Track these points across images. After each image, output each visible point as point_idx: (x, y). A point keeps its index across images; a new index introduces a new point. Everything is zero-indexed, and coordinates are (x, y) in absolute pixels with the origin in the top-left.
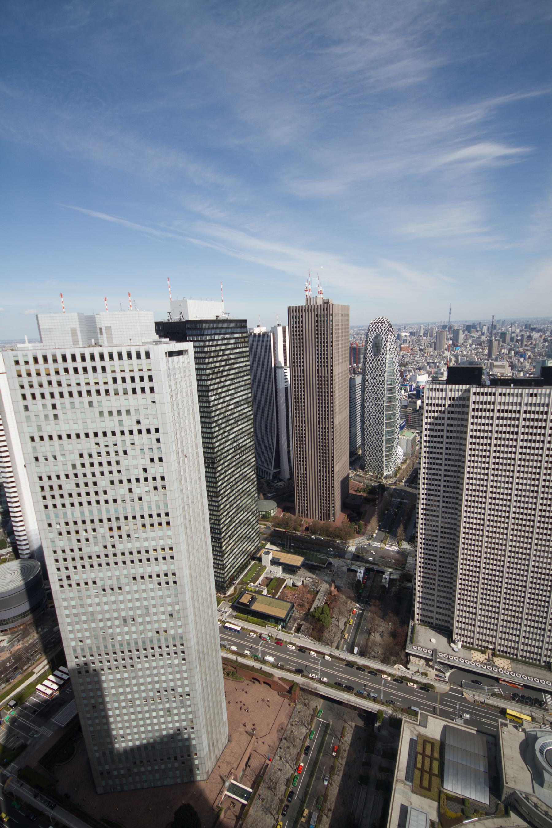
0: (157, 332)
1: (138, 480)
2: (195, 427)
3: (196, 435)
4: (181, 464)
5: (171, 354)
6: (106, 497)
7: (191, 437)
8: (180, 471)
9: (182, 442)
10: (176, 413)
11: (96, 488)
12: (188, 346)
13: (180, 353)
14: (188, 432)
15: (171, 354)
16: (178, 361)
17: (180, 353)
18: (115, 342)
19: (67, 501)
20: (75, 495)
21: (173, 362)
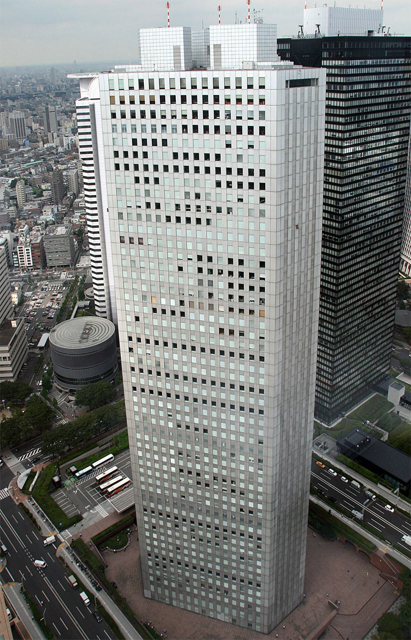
2: (315, 188)
3: (315, 200)
4: (290, 238)
5: (293, 84)
9: (294, 207)
10: (291, 165)
12: (320, 74)
14: (304, 195)
15: (293, 84)
16: (303, 95)
18: (224, 65)
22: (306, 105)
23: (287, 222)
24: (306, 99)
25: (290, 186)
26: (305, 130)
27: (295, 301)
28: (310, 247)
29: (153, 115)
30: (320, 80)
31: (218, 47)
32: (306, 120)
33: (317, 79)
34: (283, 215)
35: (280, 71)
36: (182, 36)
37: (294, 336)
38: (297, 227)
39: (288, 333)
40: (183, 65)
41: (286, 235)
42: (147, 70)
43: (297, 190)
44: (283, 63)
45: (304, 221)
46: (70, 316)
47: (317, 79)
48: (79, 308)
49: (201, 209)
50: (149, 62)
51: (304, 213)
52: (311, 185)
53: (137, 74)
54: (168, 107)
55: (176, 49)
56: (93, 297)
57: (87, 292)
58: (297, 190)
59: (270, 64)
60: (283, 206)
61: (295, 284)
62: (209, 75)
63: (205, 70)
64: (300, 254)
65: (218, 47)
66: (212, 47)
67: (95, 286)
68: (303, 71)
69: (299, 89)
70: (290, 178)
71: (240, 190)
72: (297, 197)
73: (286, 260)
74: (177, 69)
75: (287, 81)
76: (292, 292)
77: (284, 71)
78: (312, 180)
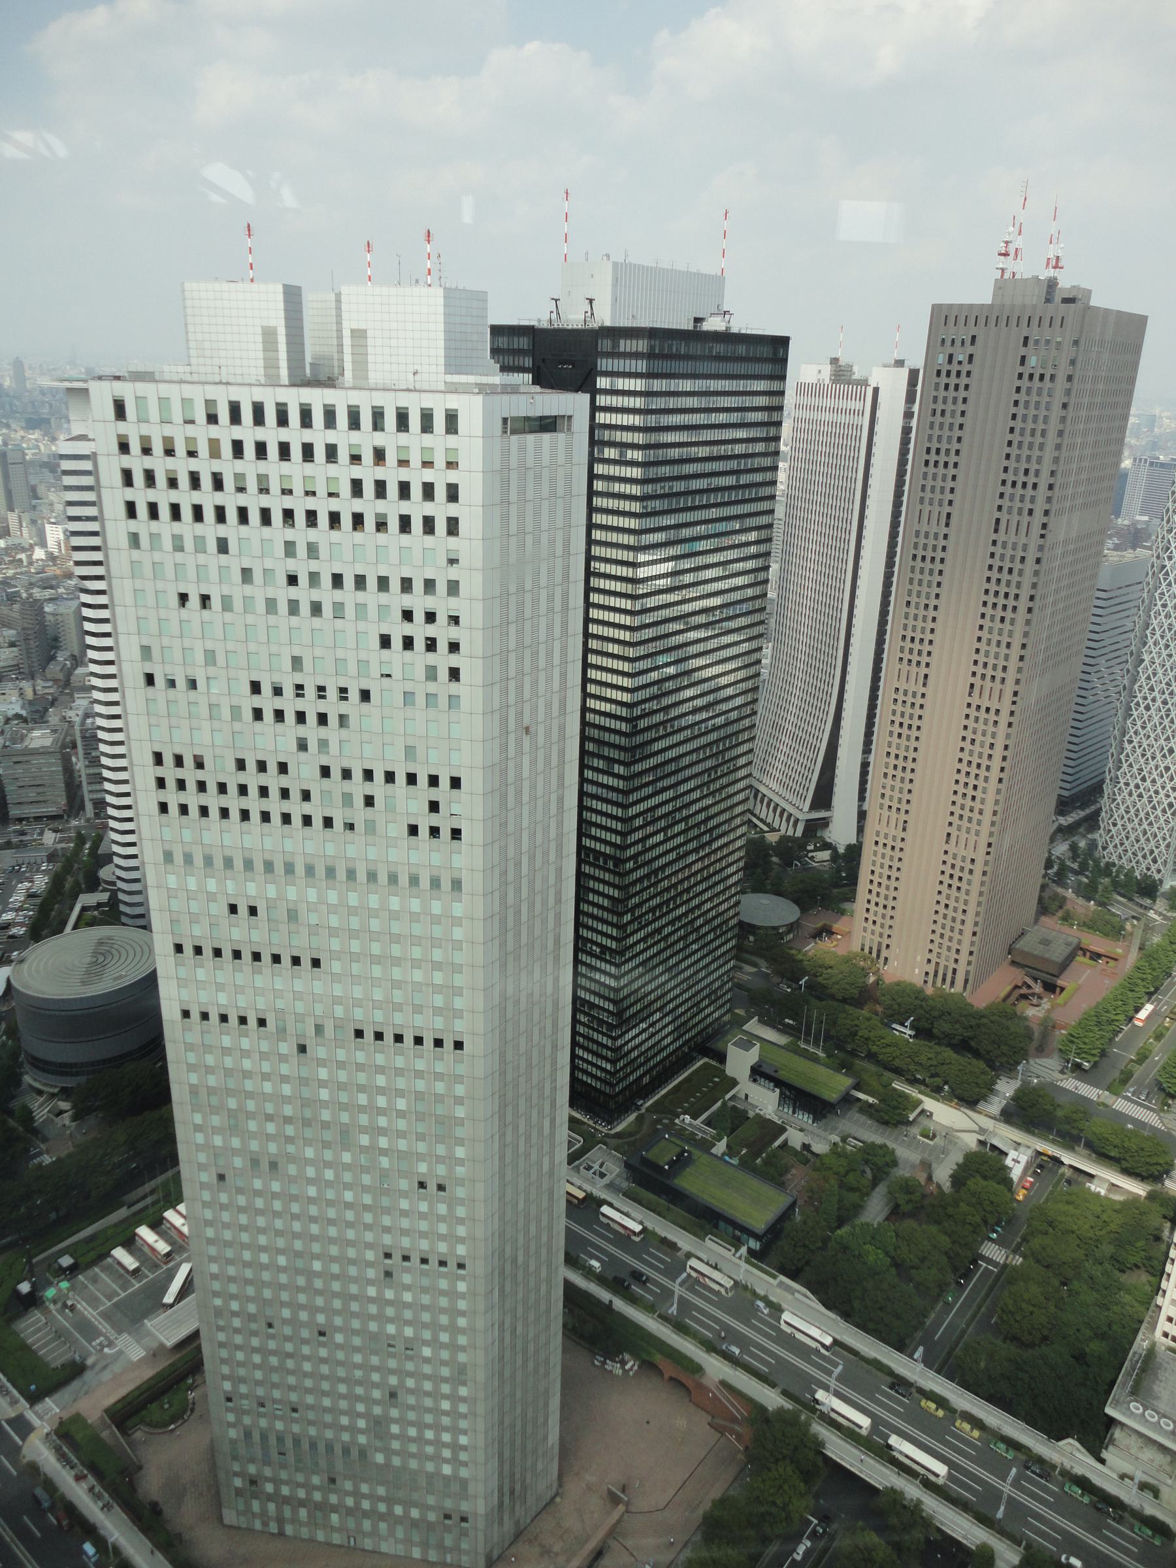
0: (495, 352)
1: (390, 777)
3: (564, 675)
6: (307, 809)
7: (549, 679)
8: (504, 773)
9: (520, 688)
11: (284, 781)
12: (574, 404)
13: (548, 424)
14: (542, 663)
16: (538, 448)
17: (548, 424)
18: (374, 378)
19: (213, 801)
20: (232, 789)
22: (546, 474)
23: (504, 720)
24: (546, 461)
26: (545, 525)
27: (525, 881)
28: (554, 773)
29: (218, 484)
30: (575, 421)
31: (359, 335)
32: (545, 504)
33: (570, 417)
34: (497, 706)
35: (491, 397)
36: (281, 306)
37: (524, 952)
38: (527, 729)
39: (510, 946)
40: (284, 373)
41: (504, 748)
42: (203, 379)
43: (527, 653)
44: (497, 379)
45: (541, 717)
46: (64, 923)
47: (570, 417)
48: (84, 909)
49: (328, 693)
50: (208, 361)
51: (541, 702)
53: (176, 386)
54: (249, 465)
55: (269, 335)
56: (114, 884)
57: (105, 873)
58: (527, 653)
60: (497, 688)
62: (340, 399)
63: (334, 386)
64: (533, 787)
65: (359, 335)
66: (346, 333)
67: (116, 860)
68: (538, 398)
69: (531, 438)
70: (512, 629)
71: (408, 653)
72: (527, 669)
73: (504, 797)
74: (272, 381)
76: (518, 865)
77: (497, 398)
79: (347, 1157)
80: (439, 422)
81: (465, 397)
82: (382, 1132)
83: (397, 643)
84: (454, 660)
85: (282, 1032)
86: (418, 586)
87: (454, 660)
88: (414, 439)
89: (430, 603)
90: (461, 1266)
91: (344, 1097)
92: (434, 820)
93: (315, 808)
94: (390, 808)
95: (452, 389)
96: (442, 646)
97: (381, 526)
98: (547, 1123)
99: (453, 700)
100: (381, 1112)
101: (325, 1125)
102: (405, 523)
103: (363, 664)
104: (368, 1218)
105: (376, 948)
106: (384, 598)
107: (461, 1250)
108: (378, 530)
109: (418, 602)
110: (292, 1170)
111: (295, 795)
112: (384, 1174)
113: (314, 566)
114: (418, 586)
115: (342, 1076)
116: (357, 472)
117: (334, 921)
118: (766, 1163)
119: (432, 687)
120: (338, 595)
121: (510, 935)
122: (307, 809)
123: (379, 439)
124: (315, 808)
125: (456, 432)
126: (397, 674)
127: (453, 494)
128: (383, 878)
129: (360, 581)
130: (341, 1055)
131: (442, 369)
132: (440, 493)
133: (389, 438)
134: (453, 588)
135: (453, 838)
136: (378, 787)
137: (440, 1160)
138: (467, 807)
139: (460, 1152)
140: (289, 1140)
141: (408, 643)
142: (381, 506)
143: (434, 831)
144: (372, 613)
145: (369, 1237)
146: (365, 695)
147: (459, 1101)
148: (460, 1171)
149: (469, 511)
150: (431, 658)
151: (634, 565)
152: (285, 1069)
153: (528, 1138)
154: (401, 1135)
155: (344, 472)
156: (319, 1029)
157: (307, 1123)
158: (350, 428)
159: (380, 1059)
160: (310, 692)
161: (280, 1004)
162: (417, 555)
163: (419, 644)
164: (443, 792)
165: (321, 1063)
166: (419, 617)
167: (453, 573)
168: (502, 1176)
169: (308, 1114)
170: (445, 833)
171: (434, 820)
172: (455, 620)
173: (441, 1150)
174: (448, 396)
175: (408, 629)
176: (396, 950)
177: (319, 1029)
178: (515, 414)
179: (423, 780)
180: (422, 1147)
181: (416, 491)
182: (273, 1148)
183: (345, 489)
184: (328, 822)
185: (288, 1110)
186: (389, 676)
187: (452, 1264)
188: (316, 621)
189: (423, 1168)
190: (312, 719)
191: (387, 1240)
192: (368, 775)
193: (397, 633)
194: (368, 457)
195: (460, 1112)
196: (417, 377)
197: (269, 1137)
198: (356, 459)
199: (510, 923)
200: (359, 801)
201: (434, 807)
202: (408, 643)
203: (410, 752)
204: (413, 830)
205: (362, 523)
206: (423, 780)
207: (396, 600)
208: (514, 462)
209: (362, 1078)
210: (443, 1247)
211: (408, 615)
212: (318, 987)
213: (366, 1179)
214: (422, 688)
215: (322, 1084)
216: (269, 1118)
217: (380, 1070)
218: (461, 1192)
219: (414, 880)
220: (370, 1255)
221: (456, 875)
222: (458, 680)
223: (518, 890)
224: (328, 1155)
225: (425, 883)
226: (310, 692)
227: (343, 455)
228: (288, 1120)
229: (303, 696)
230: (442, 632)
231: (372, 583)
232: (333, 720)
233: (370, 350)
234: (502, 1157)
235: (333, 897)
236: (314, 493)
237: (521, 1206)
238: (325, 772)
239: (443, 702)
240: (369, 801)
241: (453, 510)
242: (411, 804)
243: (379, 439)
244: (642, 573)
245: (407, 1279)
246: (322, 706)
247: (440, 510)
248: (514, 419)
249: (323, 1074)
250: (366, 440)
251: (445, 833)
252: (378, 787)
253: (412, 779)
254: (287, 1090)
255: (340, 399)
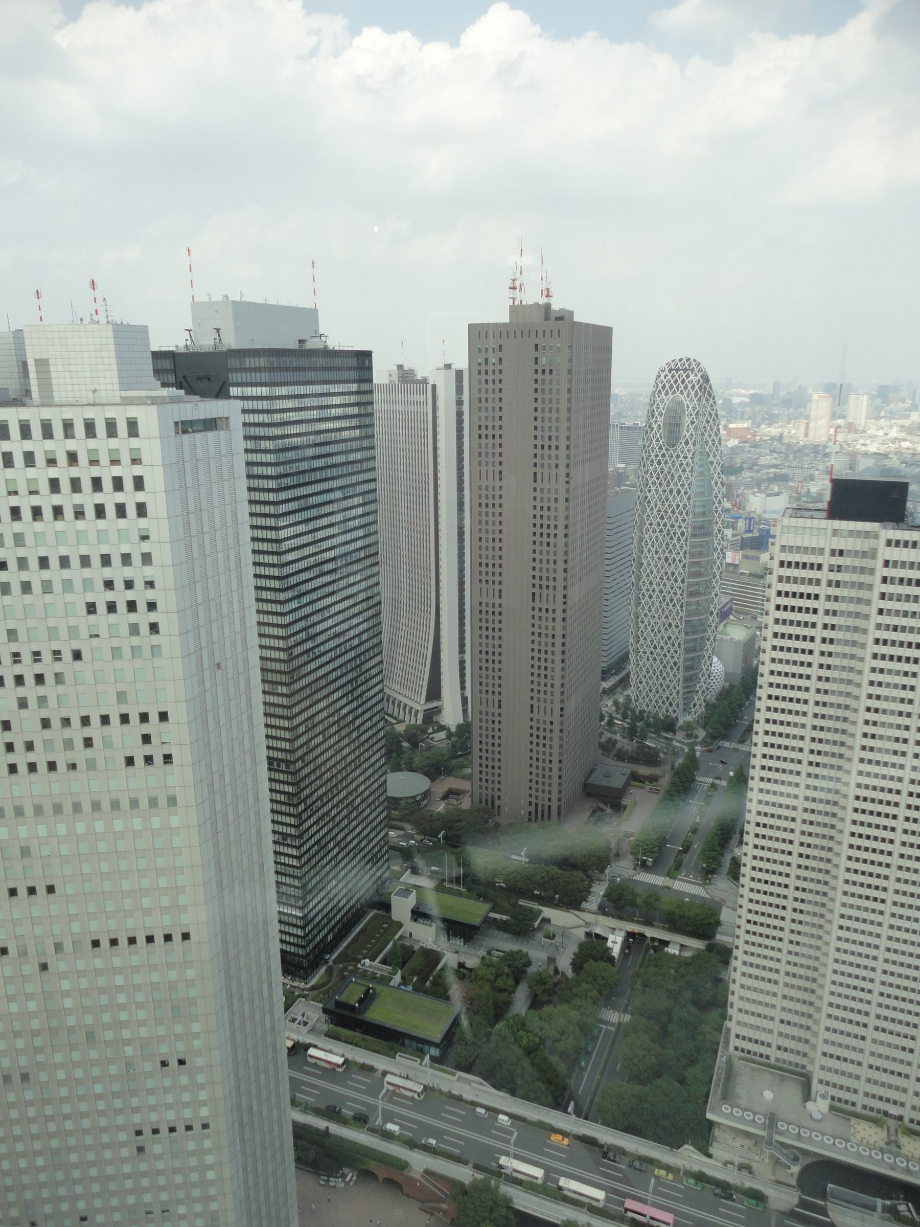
0: (157, 372)
1: (105, 720)
2: (241, 598)
3: (243, 619)
4: (208, 685)
5: (185, 427)
6: (31, 757)
9: (210, 633)
10: (196, 563)
12: (228, 409)
13: (210, 424)
14: (225, 612)
15: (185, 427)
17: (210, 424)
18: (58, 397)
21: (193, 445)
24: (212, 453)
25: (200, 600)
26: (216, 502)
27: (228, 789)
28: (243, 697)
31: (42, 364)
34: (192, 649)
38: (218, 664)
41: (202, 682)
44: (165, 392)
47: (227, 418)
52: (235, 595)
59: (143, 393)
61: (226, 761)
62: (33, 415)
68: (201, 405)
69: (198, 436)
73: (205, 723)
75: (176, 423)
76: (222, 776)
77: (169, 407)
78: (234, 586)
79: (93, 1054)
80: (122, 429)
81: (143, 408)
82: (123, 1024)
83: (102, 608)
84: (153, 617)
85: (23, 953)
86: (116, 560)
87: (153, 617)
88: (102, 444)
89: (128, 573)
90: (205, 1126)
91: (87, 1002)
92: (148, 750)
93: (40, 757)
94: (108, 743)
95: (128, 402)
96: (142, 606)
97: (79, 514)
98: (265, 987)
99: (155, 650)
100: (122, 1007)
101: (71, 1030)
102: (100, 511)
103: (73, 631)
104: (118, 1103)
105: (105, 867)
106: (87, 573)
107: (204, 1112)
108: (76, 518)
109: (118, 573)
110: (43, 1076)
111: (19, 747)
112: (129, 1065)
113: (21, 552)
114: (116, 560)
115: (84, 983)
116: (53, 473)
117: (65, 850)
118: (434, 984)
119: (135, 641)
120: (45, 574)
121: (221, 835)
122: (31, 757)
123: (71, 445)
124: (40, 757)
125: (137, 436)
126: (104, 633)
127: (139, 484)
128: (106, 805)
129: (64, 562)
130: (81, 965)
131: (117, 387)
132: (128, 484)
133: (80, 444)
134: (147, 558)
135: (165, 763)
136: (95, 730)
137: (178, 1038)
138: (175, 736)
139: (196, 1027)
140: (38, 1050)
141: (112, 608)
142: (77, 499)
143: (149, 759)
144: (78, 586)
145: (120, 1120)
146: (77, 655)
147: (190, 984)
148: (197, 1043)
149: (156, 496)
150: (133, 618)
151: (276, 529)
152: (29, 988)
153: (252, 1002)
154: (142, 1023)
155: (41, 474)
156: (58, 947)
157: (53, 1032)
158: (45, 438)
159: (117, 962)
160: (26, 658)
161: (20, 931)
162: (116, 535)
163: (122, 607)
164: (153, 726)
165: (62, 976)
166: (119, 585)
167: (146, 547)
168: (233, 1040)
169: (54, 1023)
170: (158, 759)
171: (148, 750)
172: (150, 584)
173: (178, 1029)
174: (128, 407)
175: (110, 596)
176: (123, 865)
177: (58, 947)
178: (183, 419)
179: (134, 719)
180: (161, 1031)
181: (107, 484)
182: (23, 1061)
183: (45, 487)
184: (52, 766)
185: (35, 1024)
186: (97, 636)
187: (197, 1127)
188: (27, 598)
189: (164, 1049)
190: (29, 680)
191: (137, 1119)
192: (85, 721)
193: (102, 598)
194: (62, 460)
195: (193, 993)
196: (96, 394)
197: (19, 1052)
198: (52, 462)
199: (220, 825)
200: (79, 744)
201: (146, 739)
202: (112, 608)
203: (121, 697)
204: (130, 761)
205: (62, 514)
206: (134, 719)
207: (99, 573)
208: (187, 456)
209: (101, 981)
210: (188, 1114)
211: (109, 585)
212: (54, 910)
213: (113, 1070)
214: (126, 642)
215: (65, 994)
216: (17, 1035)
217: (117, 971)
218: (199, 1062)
219: (134, 803)
220: (123, 1136)
221: (171, 793)
222: (157, 632)
223: (224, 796)
224: (76, 1056)
225: (144, 803)
226: (26, 658)
227: (40, 460)
228: (35, 1033)
229: (20, 662)
230: (140, 595)
231: (75, 562)
232: (49, 679)
233: (53, 375)
234: (232, 1024)
235: (62, 829)
236: (16, 493)
237: (251, 1062)
238: (46, 724)
239: (147, 652)
240: (88, 742)
241: (140, 497)
242: (127, 739)
243: (71, 445)
244: (284, 534)
245: (158, 1149)
246: (38, 669)
247: (129, 497)
248: (183, 423)
249: (65, 985)
250: (59, 446)
251: (158, 759)
252: (95, 730)
253: (125, 719)
254: (32, 1006)
255: (33, 415)
